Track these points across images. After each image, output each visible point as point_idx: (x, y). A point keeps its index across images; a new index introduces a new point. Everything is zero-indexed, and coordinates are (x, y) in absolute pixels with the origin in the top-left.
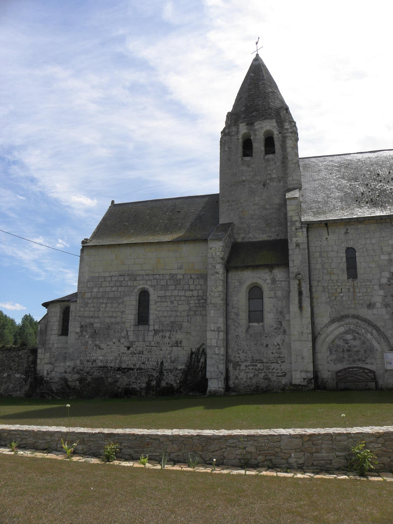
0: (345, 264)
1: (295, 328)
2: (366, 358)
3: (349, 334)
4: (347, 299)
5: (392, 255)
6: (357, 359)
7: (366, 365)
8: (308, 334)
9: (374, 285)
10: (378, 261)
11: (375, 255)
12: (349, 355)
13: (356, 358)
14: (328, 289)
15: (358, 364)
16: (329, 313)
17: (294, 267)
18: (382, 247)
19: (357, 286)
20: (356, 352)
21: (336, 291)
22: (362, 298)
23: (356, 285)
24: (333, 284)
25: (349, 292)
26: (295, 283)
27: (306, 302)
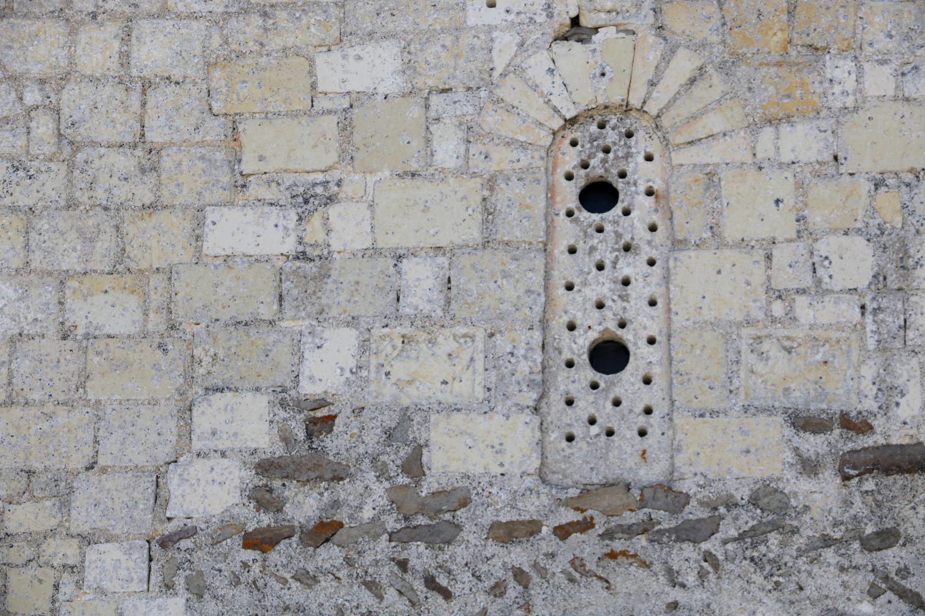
5: (333, 211)
9: (87, 540)
10: (170, 273)
11: (151, 208)
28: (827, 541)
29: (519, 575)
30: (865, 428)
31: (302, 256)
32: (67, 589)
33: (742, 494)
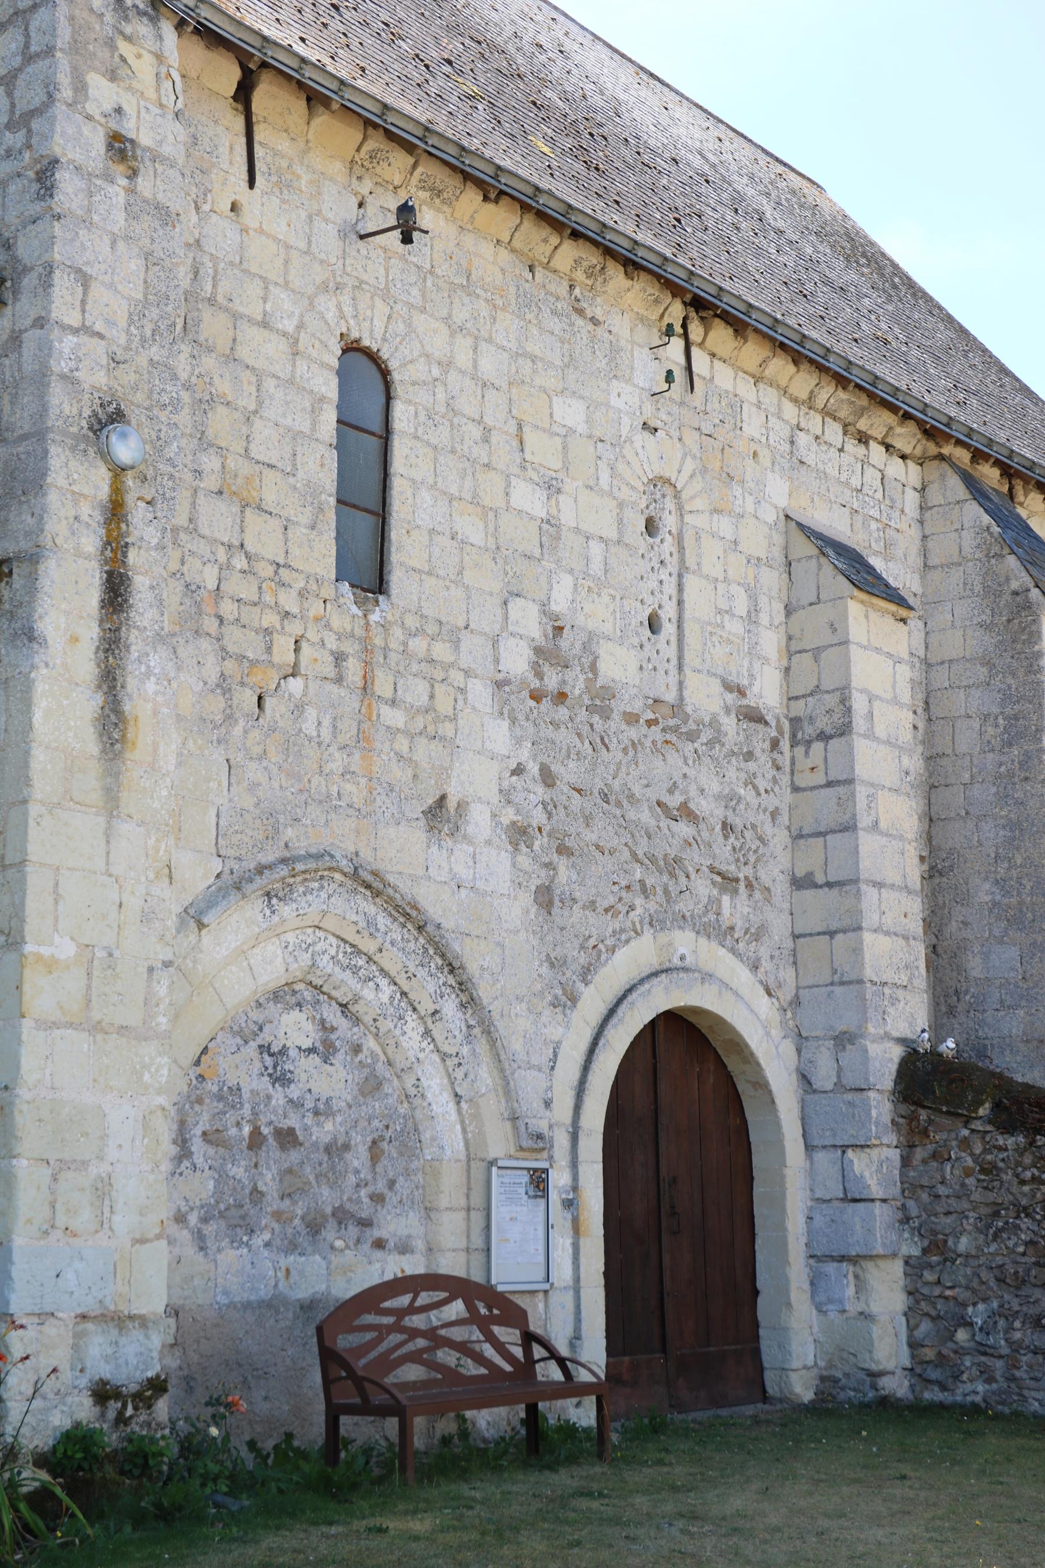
0: (332, 459)
1: (57, 899)
2: (378, 1199)
3: (299, 1005)
4: (326, 733)
5: (561, 498)
6: (329, 1210)
7: (378, 1254)
8: (151, 970)
12: (290, 1171)
13: (327, 1197)
14: (221, 620)
15: (332, 1247)
16: (213, 813)
17: (84, 339)
18: (520, 427)
19: (386, 649)
20: (328, 1149)
21: (269, 649)
22: (402, 744)
23: (378, 641)
24: (247, 591)
25: (339, 680)
26: (85, 491)
27: (151, 686)
28: (733, 753)
29: (633, 743)
30: (741, 692)
31: (548, 522)
32: (460, 703)
33: (707, 720)
